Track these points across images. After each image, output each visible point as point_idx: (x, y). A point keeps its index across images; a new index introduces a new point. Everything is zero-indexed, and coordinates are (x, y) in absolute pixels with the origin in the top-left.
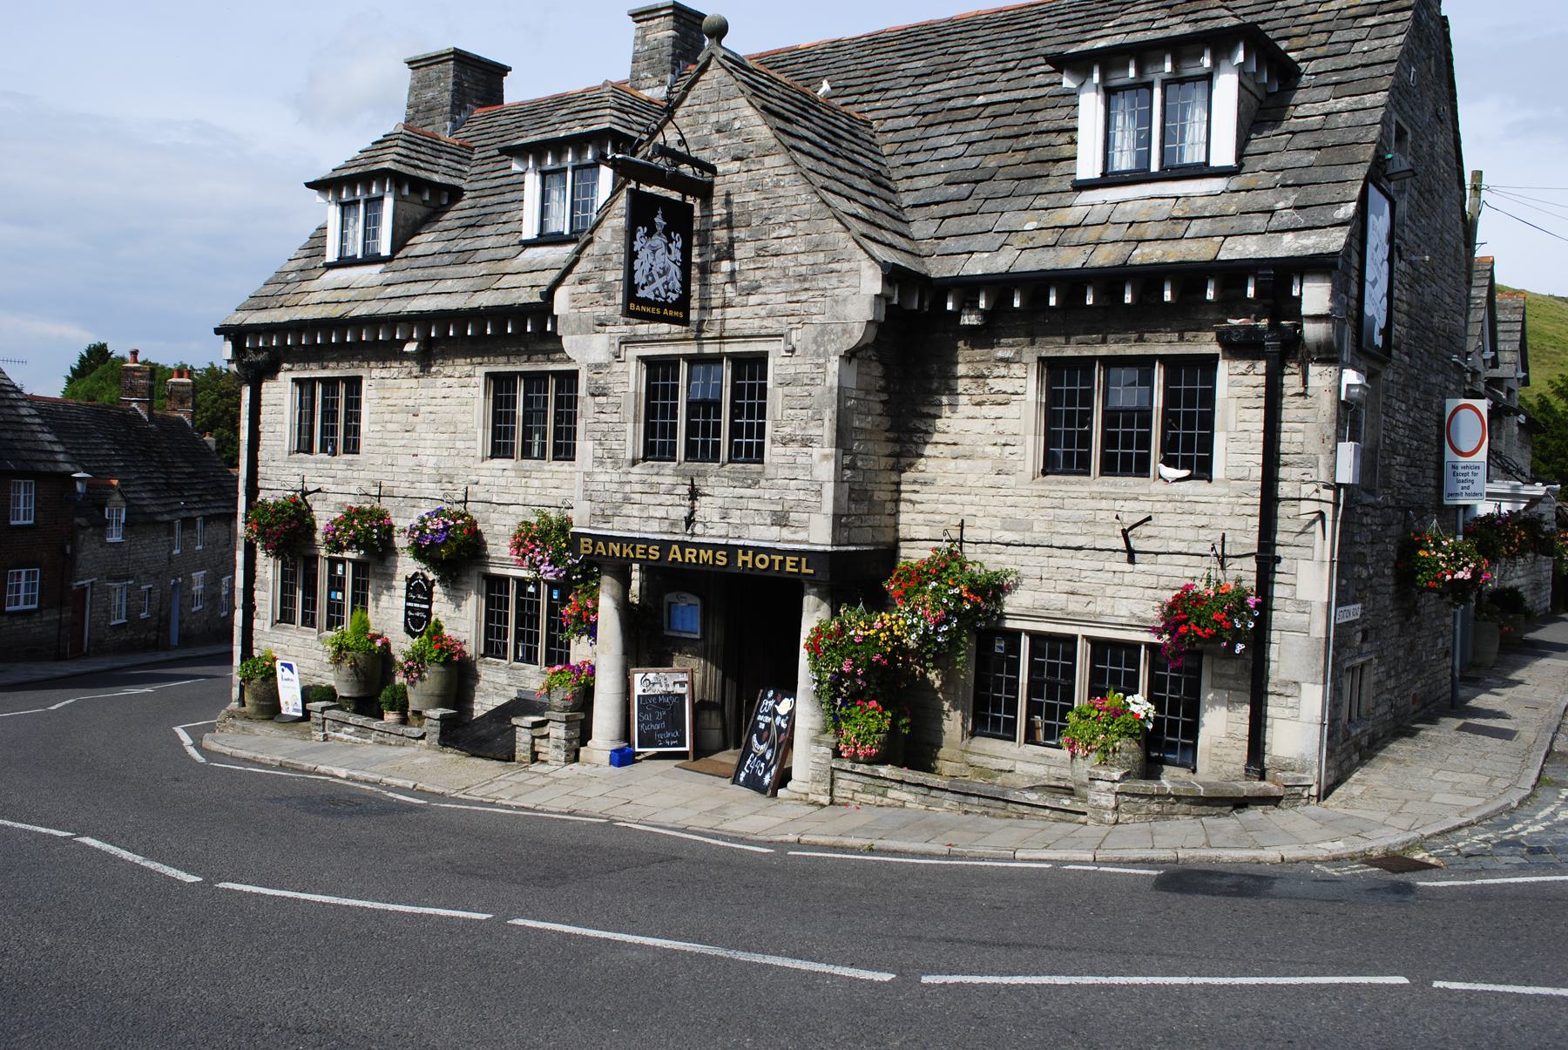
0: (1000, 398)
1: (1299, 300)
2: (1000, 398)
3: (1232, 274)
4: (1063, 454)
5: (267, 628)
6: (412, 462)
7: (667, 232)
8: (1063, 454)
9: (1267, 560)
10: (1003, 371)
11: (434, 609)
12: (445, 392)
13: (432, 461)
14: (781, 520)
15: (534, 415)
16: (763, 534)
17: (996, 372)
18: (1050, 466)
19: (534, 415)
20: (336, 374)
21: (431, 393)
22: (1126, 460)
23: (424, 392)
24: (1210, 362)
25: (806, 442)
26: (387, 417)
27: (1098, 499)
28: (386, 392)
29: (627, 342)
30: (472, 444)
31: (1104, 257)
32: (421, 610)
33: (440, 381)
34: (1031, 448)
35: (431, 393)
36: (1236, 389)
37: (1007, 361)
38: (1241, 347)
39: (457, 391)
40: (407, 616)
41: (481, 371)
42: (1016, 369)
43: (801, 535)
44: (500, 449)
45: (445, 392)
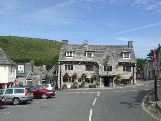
3: (132, 63)
8: (124, 70)
9: (133, 75)
14: (113, 74)
16: (112, 75)
18: (123, 71)
22: (127, 71)
24: (130, 67)
27: (126, 72)
31: (127, 62)
36: (132, 68)
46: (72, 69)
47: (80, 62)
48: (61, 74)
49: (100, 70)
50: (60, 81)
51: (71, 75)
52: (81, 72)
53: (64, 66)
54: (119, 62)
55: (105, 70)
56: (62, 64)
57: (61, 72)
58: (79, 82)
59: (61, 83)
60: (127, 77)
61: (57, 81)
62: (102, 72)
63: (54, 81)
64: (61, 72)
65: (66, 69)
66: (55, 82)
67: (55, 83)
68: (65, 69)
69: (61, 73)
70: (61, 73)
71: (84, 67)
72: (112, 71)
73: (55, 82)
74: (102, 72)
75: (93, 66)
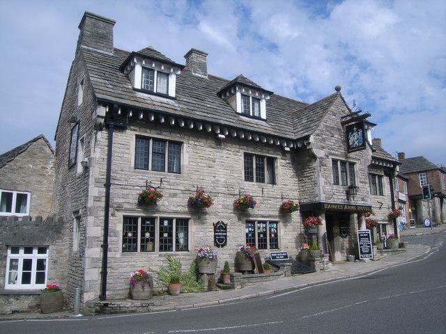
5: (119, 254)
6: (213, 179)
7: (357, 130)
11: (228, 234)
13: (223, 180)
14: (363, 199)
15: (260, 169)
19: (260, 169)
20: (167, 138)
21: (221, 155)
23: (218, 154)
25: (365, 183)
26: (198, 160)
28: (193, 153)
29: (331, 154)
32: (223, 236)
33: (225, 152)
35: (221, 155)
38: (386, 174)
39: (232, 156)
40: (215, 239)
41: (242, 152)
44: (248, 177)
46: (176, 169)
47: (223, 128)
50: (105, 248)
51: (173, 204)
52: (227, 186)
53: (127, 140)
56: (122, 129)
58: (218, 246)
59: (109, 254)
61: (185, 225)
63: (15, 250)
65: (141, 164)
66: (28, 256)
67: (41, 264)
68: (133, 164)
69: (108, 186)
70: (108, 186)
71: (231, 160)
73: (28, 256)
74: (328, 188)
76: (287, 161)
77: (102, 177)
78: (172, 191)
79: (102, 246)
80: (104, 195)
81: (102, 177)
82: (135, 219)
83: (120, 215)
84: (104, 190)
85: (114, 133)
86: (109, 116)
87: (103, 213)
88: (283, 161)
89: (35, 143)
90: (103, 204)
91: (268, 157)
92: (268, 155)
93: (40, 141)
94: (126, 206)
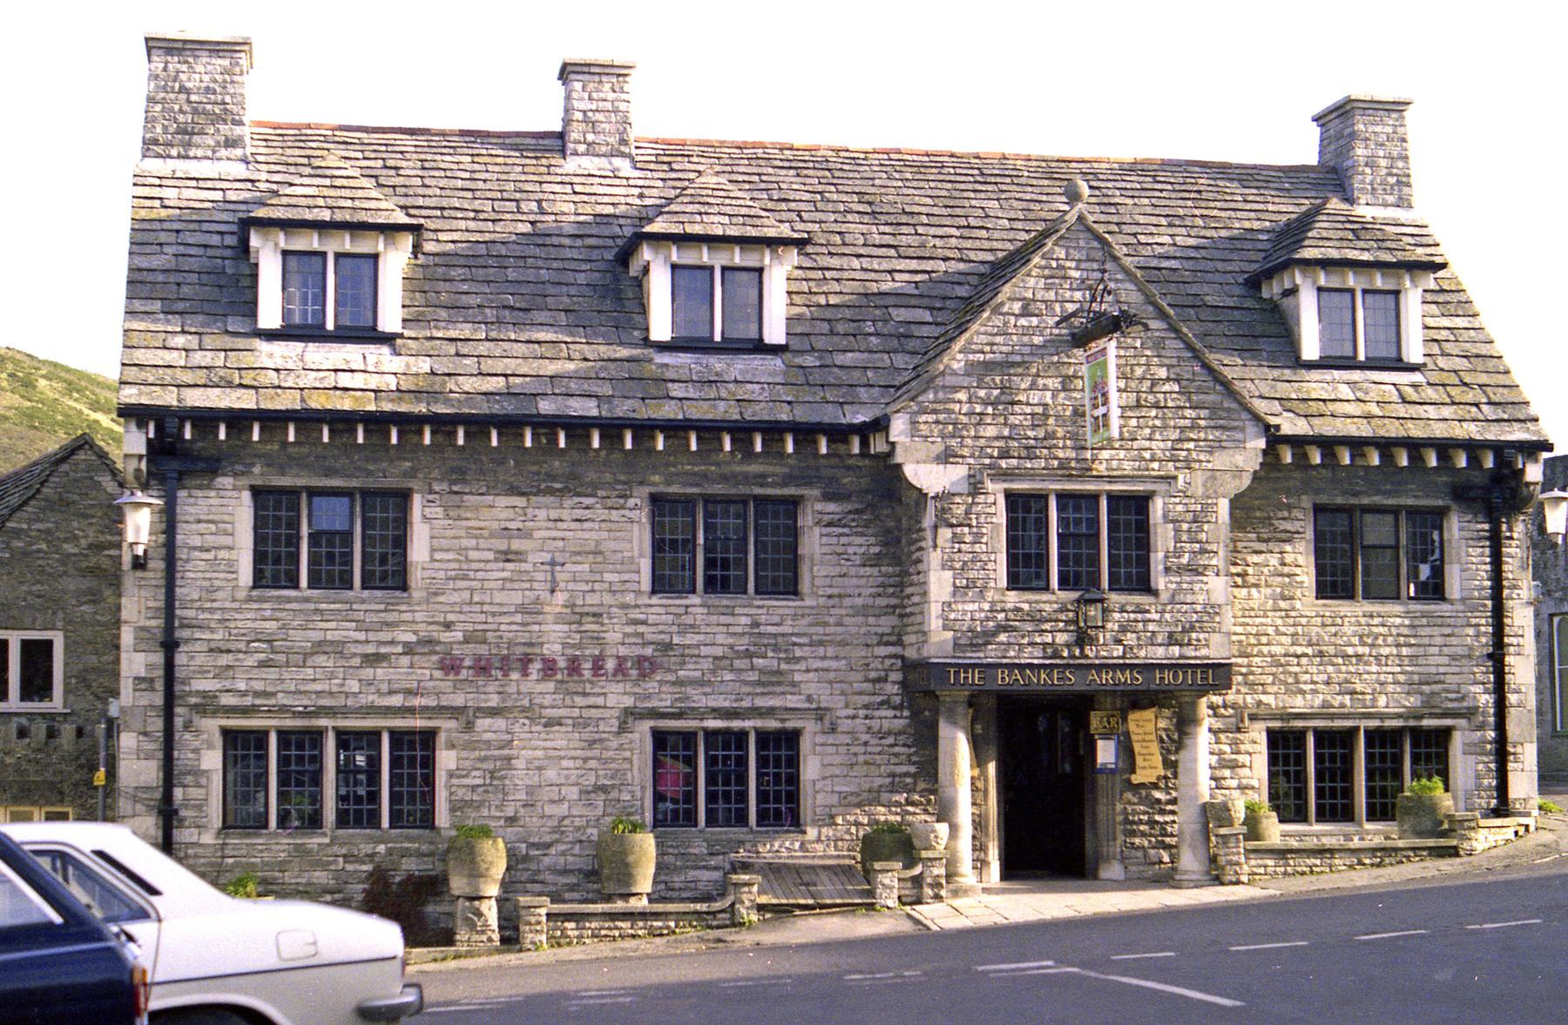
0: (1284, 536)
1: (1522, 471)
2: (1284, 536)
4: (1333, 585)
8: (1333, 585)
10: (1286, 514)
12: (578, 513)
17: (1280, 515)
24: (1442, 513)
26: (465, 543)
30: (635, 577)
34: (1307, 577)
37: (1289, 507)
39: (602, 514)
42: (1297, 513)
43: (1204, 652)
45: (578, 513)
46: (390, 572)
48: (169, 666)
49: (939, 584)
54: (1275, 439)
55: (1025, 569)
57: (169, 628)
60: (1386, 697)
62: (972, 610)
64: (169, 628)
65: (273, 568)
68: (246, 575)
69: (170, 646)
72: (1160, 581)
75: (794, 503)
76: (849, 507)
77: (154, 623)
78: (371, 649)
79: (160, 812)
80: (161, 672)
81: (154, 623)
82: (260, 737)
83: (212, 726)
84: (158, 658)
85: (182, 494)
86: (159, 450)
87: (157, 725)
88: (832, 507)
89: (64, 467)
90: (159, 699)
91: (756, 498)
92: (758, 491)
93: (81, 456)
94: (227, 700)
